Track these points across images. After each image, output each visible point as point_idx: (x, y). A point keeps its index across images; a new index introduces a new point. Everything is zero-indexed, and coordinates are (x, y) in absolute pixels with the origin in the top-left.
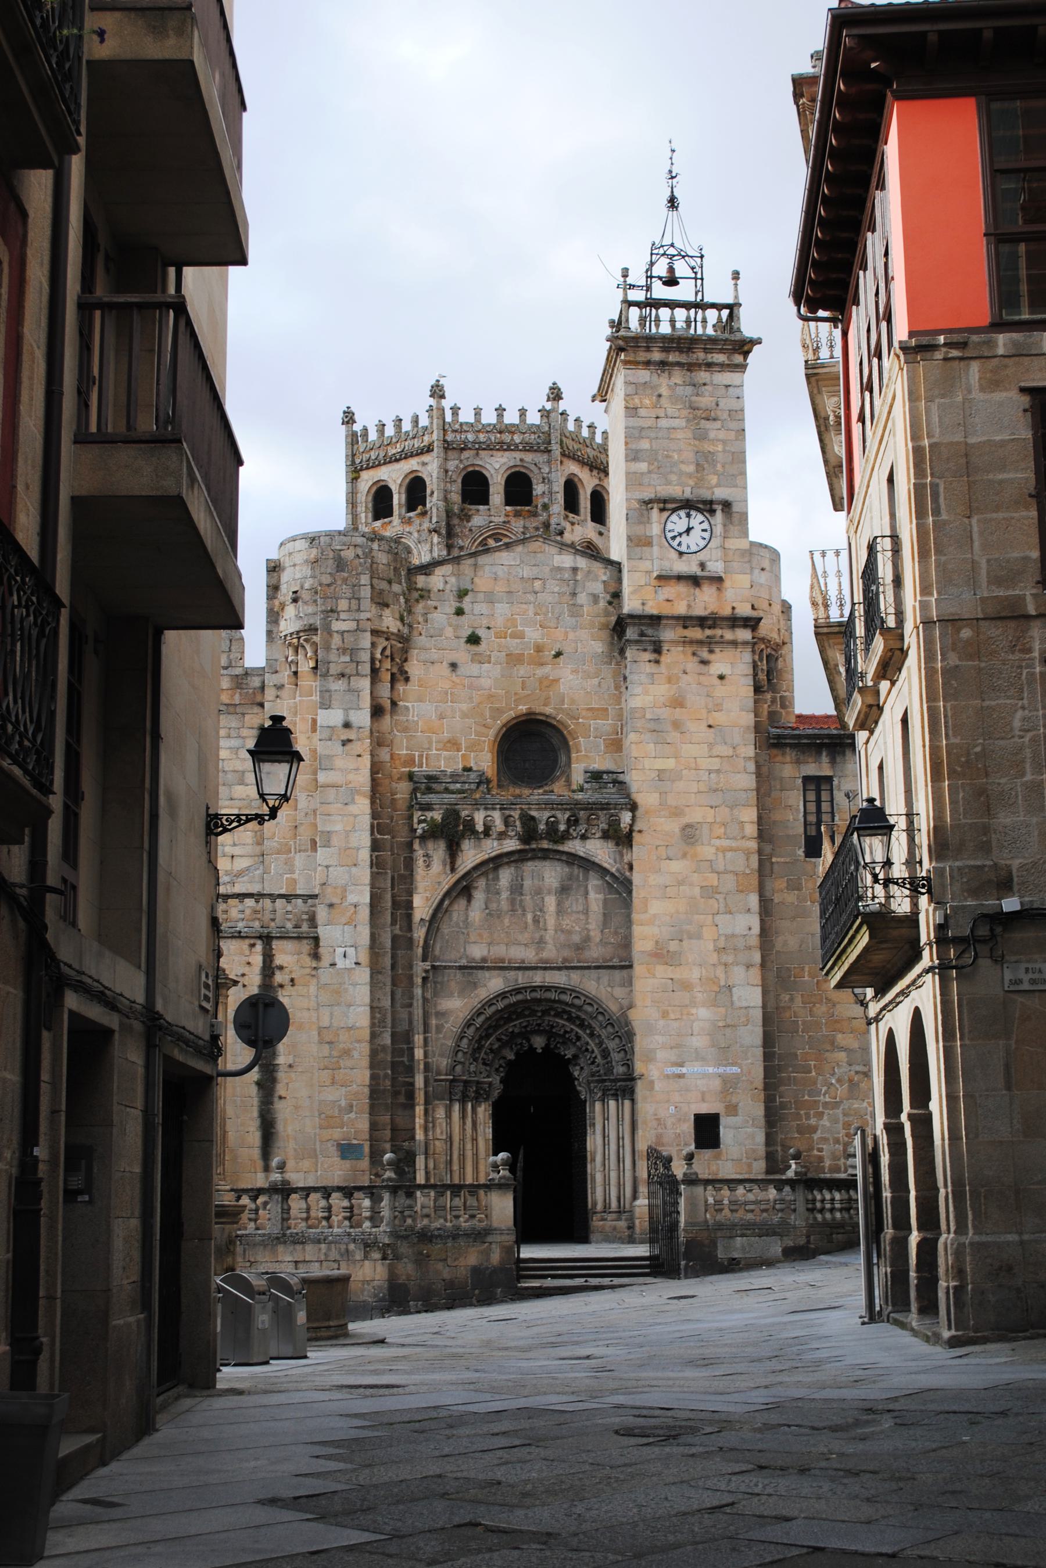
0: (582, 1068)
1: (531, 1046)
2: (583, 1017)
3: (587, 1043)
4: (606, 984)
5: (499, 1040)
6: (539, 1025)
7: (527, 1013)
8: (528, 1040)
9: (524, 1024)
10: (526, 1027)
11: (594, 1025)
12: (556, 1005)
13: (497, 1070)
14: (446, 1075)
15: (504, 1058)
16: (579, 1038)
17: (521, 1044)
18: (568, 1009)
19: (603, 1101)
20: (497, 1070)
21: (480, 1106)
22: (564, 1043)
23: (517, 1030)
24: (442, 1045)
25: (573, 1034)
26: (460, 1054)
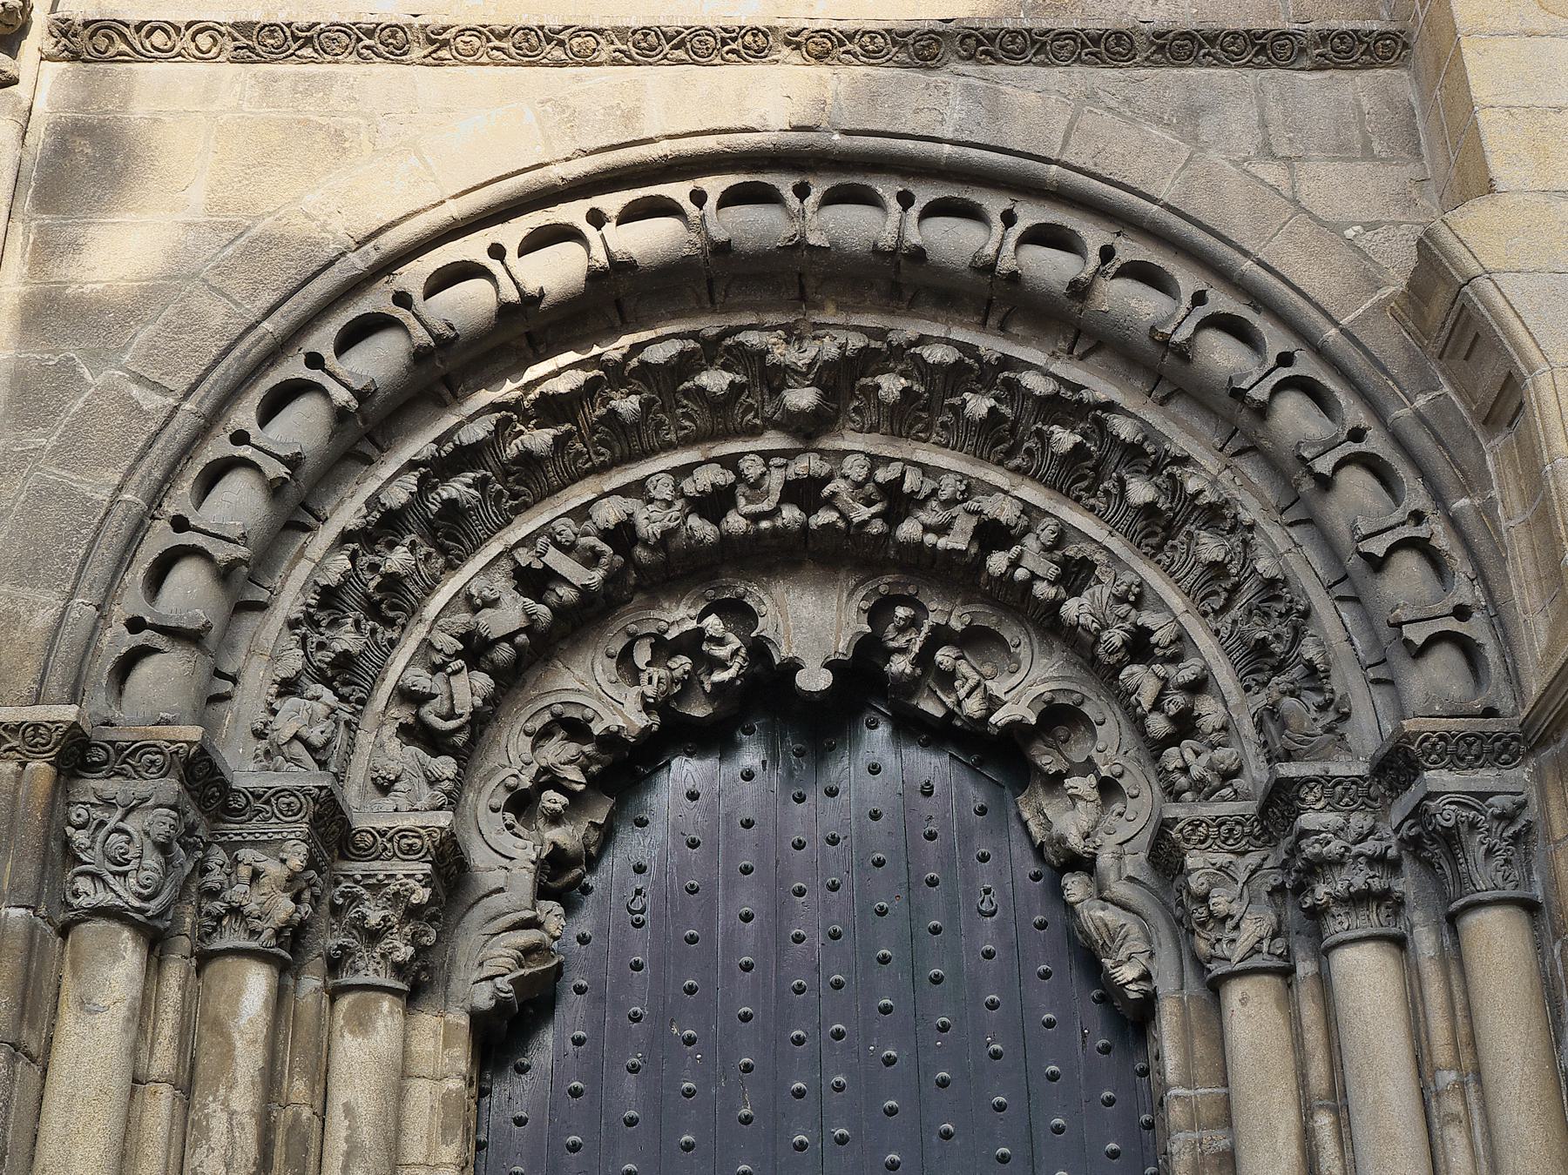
0: (1108, 788)
1: (758, 650)
2: (1099, 386)
3: (1138, 598)
4: (1248, 144)
5: (534, 582)
6: (805, 492)
7: (715, 380)
8: (739, 613)
9: (708, 478)
10: (714, 504)
11: (1180, 442)
12: (907, 329)
13: (521, 804)
14: (37, 699)
15: (576, 729)
16: (1076, 574)
17: (692, 643)
18: (991, 346)
19: (1286, 973)
20: (521, 804)
21: (361, 1023)
22: (974, 640)
23: (650, 521)
24: (45, 494)
25: (1034, 559)
26: (187, 584)
